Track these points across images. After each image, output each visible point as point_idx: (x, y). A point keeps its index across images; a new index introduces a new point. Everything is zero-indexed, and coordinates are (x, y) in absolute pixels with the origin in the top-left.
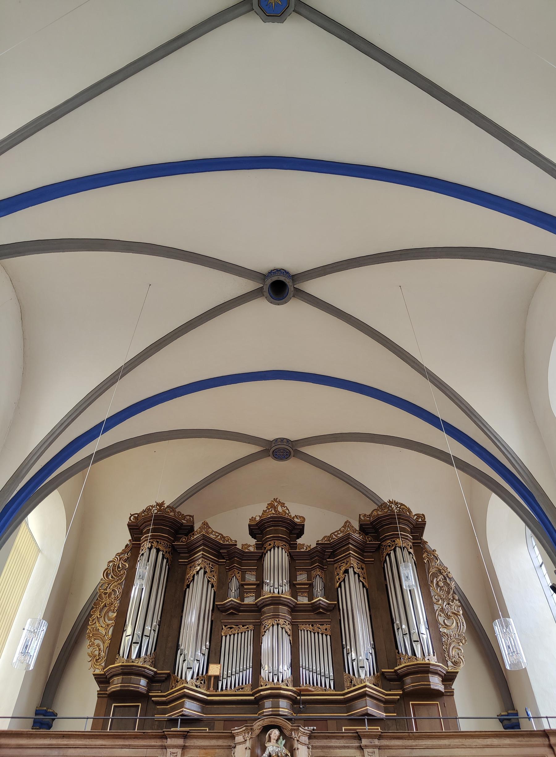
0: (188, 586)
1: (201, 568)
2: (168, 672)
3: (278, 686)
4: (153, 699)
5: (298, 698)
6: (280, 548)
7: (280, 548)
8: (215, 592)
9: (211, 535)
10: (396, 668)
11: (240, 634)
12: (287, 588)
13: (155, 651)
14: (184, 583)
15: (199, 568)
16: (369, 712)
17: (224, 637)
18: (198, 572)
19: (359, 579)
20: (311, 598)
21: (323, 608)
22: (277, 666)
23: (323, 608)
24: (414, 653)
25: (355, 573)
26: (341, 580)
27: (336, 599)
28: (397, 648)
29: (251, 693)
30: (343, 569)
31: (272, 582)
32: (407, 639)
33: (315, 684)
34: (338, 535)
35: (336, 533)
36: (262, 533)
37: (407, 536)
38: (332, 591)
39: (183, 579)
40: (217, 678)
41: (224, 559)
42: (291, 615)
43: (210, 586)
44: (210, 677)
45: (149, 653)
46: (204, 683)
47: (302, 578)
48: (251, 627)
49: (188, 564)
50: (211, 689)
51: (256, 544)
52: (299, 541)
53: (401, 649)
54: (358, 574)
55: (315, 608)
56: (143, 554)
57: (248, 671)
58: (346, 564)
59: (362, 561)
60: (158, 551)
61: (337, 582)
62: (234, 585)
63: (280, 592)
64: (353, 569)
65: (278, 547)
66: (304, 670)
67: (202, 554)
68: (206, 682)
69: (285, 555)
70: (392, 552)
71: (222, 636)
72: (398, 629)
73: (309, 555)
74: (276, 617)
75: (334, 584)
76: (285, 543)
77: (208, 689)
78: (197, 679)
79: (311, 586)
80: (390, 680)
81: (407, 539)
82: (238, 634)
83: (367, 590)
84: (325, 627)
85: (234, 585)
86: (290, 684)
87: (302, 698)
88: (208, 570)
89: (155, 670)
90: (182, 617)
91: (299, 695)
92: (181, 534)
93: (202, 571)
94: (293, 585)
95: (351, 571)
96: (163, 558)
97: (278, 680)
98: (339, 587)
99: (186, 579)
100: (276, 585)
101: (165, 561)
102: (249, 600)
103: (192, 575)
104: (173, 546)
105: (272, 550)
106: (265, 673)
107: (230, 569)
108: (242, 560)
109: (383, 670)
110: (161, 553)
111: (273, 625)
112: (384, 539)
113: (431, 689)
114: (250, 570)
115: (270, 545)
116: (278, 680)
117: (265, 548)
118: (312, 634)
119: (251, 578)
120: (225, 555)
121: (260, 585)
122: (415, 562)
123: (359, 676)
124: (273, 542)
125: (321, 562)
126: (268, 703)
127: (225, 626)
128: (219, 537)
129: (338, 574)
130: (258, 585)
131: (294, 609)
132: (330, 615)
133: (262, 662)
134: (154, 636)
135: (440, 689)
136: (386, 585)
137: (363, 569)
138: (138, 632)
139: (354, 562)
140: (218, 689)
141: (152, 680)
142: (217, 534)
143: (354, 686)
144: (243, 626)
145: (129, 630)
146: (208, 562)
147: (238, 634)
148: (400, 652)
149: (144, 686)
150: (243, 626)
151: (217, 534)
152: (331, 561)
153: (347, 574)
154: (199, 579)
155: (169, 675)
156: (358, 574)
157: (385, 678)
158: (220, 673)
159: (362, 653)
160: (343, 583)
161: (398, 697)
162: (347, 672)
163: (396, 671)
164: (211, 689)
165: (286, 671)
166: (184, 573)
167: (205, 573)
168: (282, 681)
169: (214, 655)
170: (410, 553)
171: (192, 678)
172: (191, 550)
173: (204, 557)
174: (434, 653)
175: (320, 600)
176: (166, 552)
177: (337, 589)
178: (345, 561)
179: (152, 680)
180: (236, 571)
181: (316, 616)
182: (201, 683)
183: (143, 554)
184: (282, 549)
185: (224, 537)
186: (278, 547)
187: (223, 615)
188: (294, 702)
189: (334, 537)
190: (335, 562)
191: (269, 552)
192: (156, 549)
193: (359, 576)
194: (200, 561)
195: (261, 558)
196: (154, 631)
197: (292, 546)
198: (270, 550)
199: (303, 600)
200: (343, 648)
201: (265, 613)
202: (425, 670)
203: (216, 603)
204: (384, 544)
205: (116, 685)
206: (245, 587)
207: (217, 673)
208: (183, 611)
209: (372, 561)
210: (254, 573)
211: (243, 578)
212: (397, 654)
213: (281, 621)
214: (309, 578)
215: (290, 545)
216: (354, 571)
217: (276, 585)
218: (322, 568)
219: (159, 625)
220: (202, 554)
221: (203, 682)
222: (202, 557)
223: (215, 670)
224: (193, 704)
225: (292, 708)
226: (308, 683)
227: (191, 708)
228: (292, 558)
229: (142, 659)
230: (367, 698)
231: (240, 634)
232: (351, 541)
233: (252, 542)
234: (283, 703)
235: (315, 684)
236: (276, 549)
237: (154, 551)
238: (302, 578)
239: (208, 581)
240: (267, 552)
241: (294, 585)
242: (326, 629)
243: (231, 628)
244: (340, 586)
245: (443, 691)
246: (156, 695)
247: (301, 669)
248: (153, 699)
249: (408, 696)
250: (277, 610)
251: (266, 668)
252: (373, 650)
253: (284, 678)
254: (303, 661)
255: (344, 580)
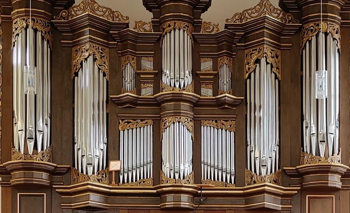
0: (76, 74)
1: (90, 55)
2: (69, 166)
3: (179, 184)
4: (57, 190)
5: (199, 192)
6: (182, 31)
7: (182, 31)
8: (107, 82)
9: (98, 12)
10: (298, 167)
11: (138, 129)
12: (189, 80)
13: (50, 145)
14: (71, 70)
15: (87, 54)
16: (266, 206)
17: (122, 132)
18: (86, 59)
19: (271, 70)
20: (216, 92)
21: (228, 104)
22: (178, 162)
23: (228, 104)
24: (318, 153)
25: (267, 63)
26: (251, 70)
27: (244, 95)
28: (303, 146)
29: (153, 187)
30: (255, 58)
31: (172, 74)
32: (314, 139)
33: (216, 179)
34: (252, 15)
35: (250, 12)
36: (159, 7)
37: (335, 18)
38: (240, 84)
39: (69, 64)
40: (118, 172)
41: (115, 40)
42: (193, 111)
43: (101, 74)
44: (111, 172)
45: (45, 148)
46: (106, 176)
47: (206, 65)
48: (150, 121)
49: (73, 46)
50: (114, 182)
51: (153, 22)
52: (205, 17)
53: (307, 149)
54: (271, 64)
55: (220, 104)
56: (18, 35)
57: (149, 166)
58: (259, 52)
59: (278, 47)
60: (35, 31)
61: (247, 72)
62: (129, 73)
63: (182, 86)
64: (266, 59)
65: (179, 29)
66: (206, 166)
67: (90, 38)
68: (107, 176)
69: (188, 43)
70: (314, 39)
71: (119, 131)
72: (307, 127)
73: (216, 38)
74: (177, 114)
75: (243, 75)
76: (187, 24)
77: (110, 183)
78: (99, 174)
79: (217, 76)
80: (291, 176)
81: (334, 22)
82: (136, 128)
83: (279, 82)
84: (229, 123)
85: (129, 73)
86: (192, 181)
87: (203, 192)
88: (98, 56)
89: (55, 165)
90: (74, 108)
91: (201, 189)
92: (59, 6)
93: (91, 58)
94: (195, 74)
95: (263, 61)
96: (43, 38)
97: (179, 177)
98: (248, 78)
99: (73, 66)
100: (177, 73)
101: (45, 43)
102: (147, 92)
103: (80, 61)
104: (52, 24)
105: (173, 32)
106: (166, 169)
107: (123, 54)
108: (136, 42)
109: (284, 168)
110: (39, 34)
111: (174, 123)
112: (307, 21)
113: (328, 187)
114: (147, 56)
115: (169, 26)
116: (179, 177)
117: (164, 29)
118: (216, 130)
119: (148, 65)
120: (116, 39)
121: (158, 73)
122: (338, 50)
123: (260, 174)
124: (173, 22)
125: (230, 48)
126: (170, 197)
127: (122, 120)
128: (107, 13)
129: (248, 63)
130: (156, 74)
131: (196, 105)
132: (235, 113)
133: (163, 158)
134: (47, 131)
135: (337, 186)
136: (302, 76)
137: (277, 57)
138: (31, 127)
139: (267, 49)
140: (119, 182)
141: (53, 173)
142: (104, 10)
143: (255, 182)
144: (142, 121)
145: (19, 125)
146: (97, 46)
147: (136, 128)
148: (305, 150)
149: (46, 180)
150: (142, 121)
151: (104, 10)
152: (242, 46)
153: (258, 65)
154: (88, 67)
155: (69, 169)
156: (271, 64)
157: (286, 174)
158: (121, 168)
159: (265, 146)
160: (252, 74)
161: (296, 192)
162: (249, 169)
163: (297, 169)
164: (114, 182)
165: (187, 168)
166: (70, 59)
167: (95, 60)
168: (184, 178)
169: (113, 150)
170: (334, 39)
171: (93, 173)
172: (75, 30)
173: (91, 41)
174: (339, 151)
175: (225, 96)
176: (46, 32)
177: (246, 80)
178: (258, 48)
179: (53, 173)
180: (131, 57)
181: (221, 112)
182: (103, 177)
183: (18, 35)
184: (184, 31)
185: (113, 12)
186: (179, 29)
187: (119, 111)
188: (194, 195)
189: (247, 16)
190: (246, 47)
191: (168, 34)
192: (33, 28)
193: (272, 67)
194: (87, 46)
195: (159, 40)
196: (47, 124)
197: (195, 24)
198: (170, 33)
199: (207, 93)
200: (247, 145)
201: (165, 109)
202: (326, 170)
203: (111, 96)
204: (306, 26)
205: (18, 178)
206: (141, 76)
207: (119, 169)
208: (74, 102)
209: (289, 46)
210: (152, 59)
211: (139, 66)
212: (302, 151)
213: (183, 119)
214: (215, 67)
215: (193, 26)
216: (266, 61)
217: (177, 73)
218: (229, 55)
219: (51, 118)
220: (90, 38)
221: (104, 176)
222: (90, 41)
223: (114, 166)
224: (97, 196)
225: (193, 201)
226: (209, 178)
227: (94, 200)
228: (195, 40)
229: (40, 156)
230: (266, 195)
231: (138, 129)
232: (266, 25)
233: (148, 16)
234: (184, 198)
235: (216, 179)
236: (177, 31)
237: (30, 31)
238: (206, 65)
239: (99, 69)
240: (166, 33)
241: (198, 75)
242: (230, 126)
243: (129, 123)
244: (249, 77)
245: (340, 187)
246: (59, 188)
247: (203, 165)
248: (57, 190)
249: (304, 191)
250: (178, 108)
251: (168, 165)
252: (278, 148)
253: (186, 175)
254: (205, 157)
255: (255, 71)
